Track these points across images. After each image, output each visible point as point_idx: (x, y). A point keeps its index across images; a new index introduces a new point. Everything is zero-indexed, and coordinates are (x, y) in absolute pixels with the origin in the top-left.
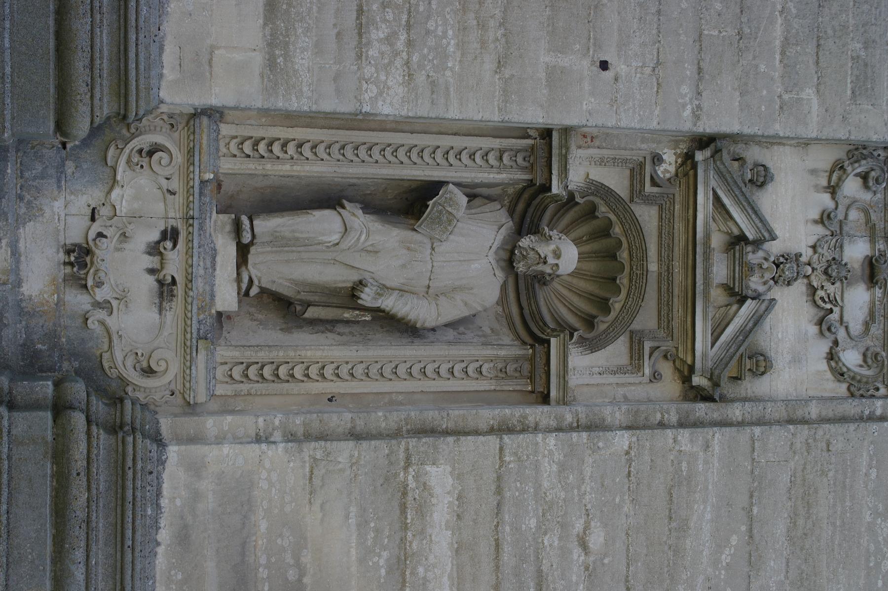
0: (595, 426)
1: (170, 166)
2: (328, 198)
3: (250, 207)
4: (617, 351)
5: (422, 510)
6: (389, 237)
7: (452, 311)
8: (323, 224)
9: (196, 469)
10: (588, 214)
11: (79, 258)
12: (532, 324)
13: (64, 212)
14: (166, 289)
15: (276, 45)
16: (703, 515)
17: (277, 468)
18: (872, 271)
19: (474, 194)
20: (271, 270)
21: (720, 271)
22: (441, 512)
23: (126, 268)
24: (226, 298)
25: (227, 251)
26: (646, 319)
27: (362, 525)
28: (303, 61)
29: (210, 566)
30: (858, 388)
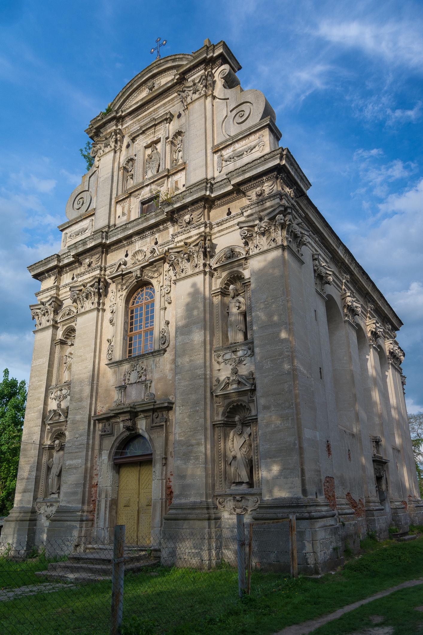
5: (70, 465)
9: (62, 500)
27: (71, 475)
29: (72, 498)
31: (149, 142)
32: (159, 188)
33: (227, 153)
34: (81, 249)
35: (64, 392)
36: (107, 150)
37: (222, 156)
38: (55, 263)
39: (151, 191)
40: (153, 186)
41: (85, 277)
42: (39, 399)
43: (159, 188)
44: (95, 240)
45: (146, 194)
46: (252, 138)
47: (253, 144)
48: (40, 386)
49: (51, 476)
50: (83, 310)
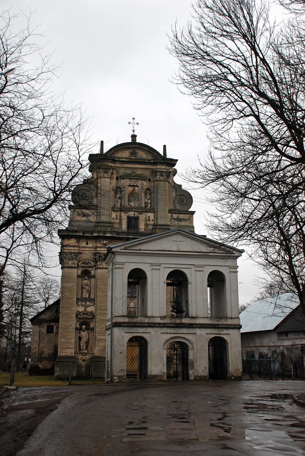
0: (96, 326)
1: (78, 355)
2: (80, 344)
3: (80, 350)
4: (91, 323)
6: (82, 340)
7: (88, 335)
8: (81, 344)
10: (81, 325)
11: (84, 360)
12: (88, 328)
13: (81, 361)
14: (86, 355)
15: (70, 348)
16: (102, 318)
17: (97, 348)
18: (86, 302)
19: (79, 333)
20: (84, 348)
21: (85, 316)
22: (100, 337)
23: (84, 357)
24: (86, 351)
25: (83, 351)
26: (88, 321)
28: (71, 346)
30: (94, 304)
31: (131, 184)
32: (139, 215)
33: (175, 216)
34: (101, 235)
35: (88, 303)
36: (106, 175)
37: (172, 216)
38: (81, 234)
39: (134, 214)
40: (136, 213)
41: (102, 249)
42: (72, 304)
43: (139, 215)
44: (112, 234)
45: (131, 214)
46: (186, 215)
47: (187, 218)
48: (72, 298)
49: (81, 342)
50: (101, 266)
